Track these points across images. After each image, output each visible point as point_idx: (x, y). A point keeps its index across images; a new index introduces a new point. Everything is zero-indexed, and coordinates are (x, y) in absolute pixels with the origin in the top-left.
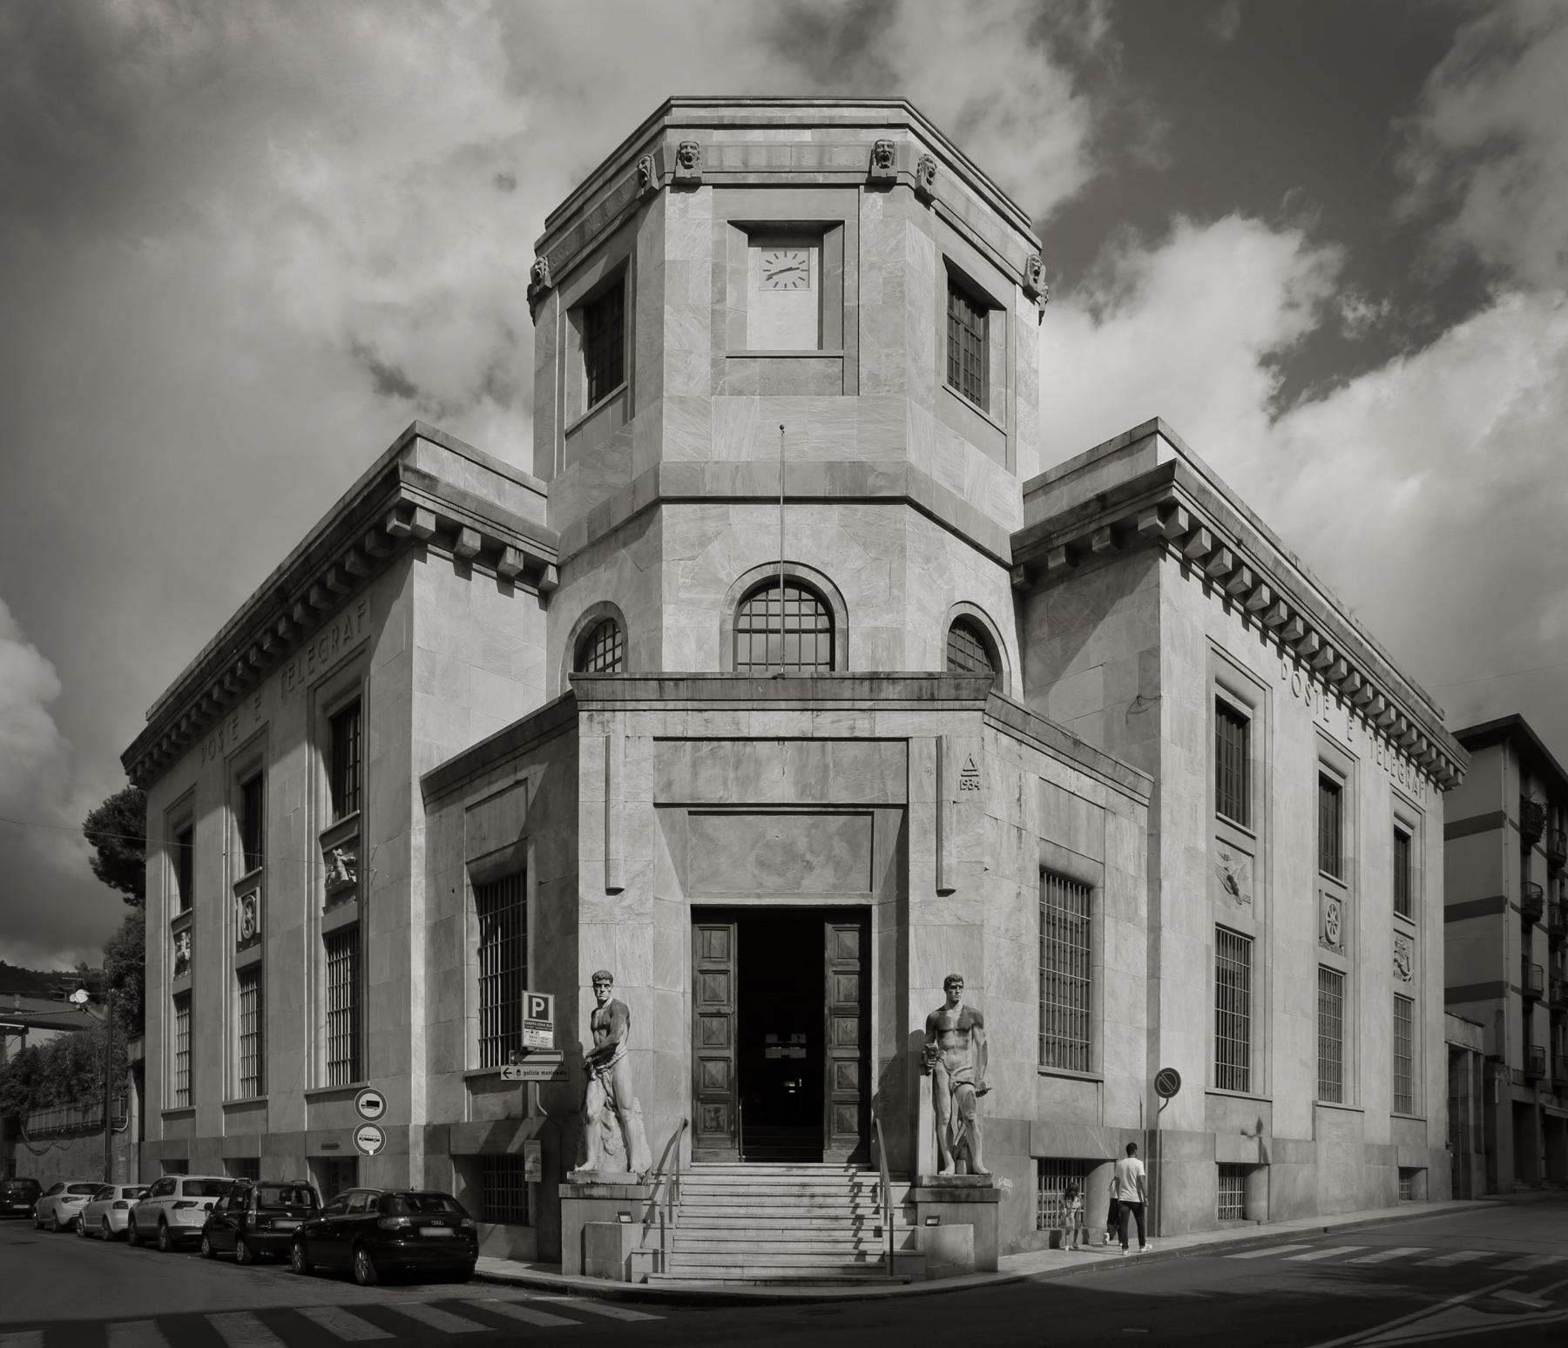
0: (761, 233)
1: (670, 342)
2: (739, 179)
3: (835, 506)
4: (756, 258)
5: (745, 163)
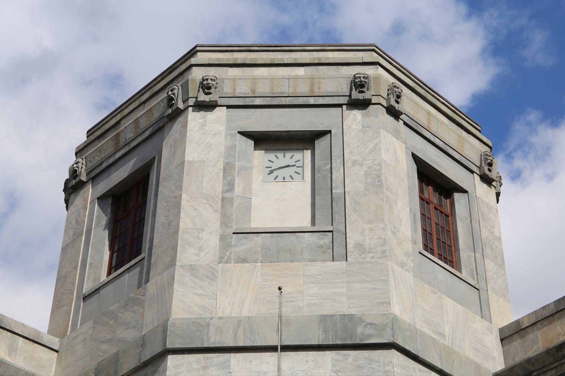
0: (263, 140)
1: (185, 222)
2: (248, 102)
3: (328, 353)
4: (260, 158)
5: (253, 91)
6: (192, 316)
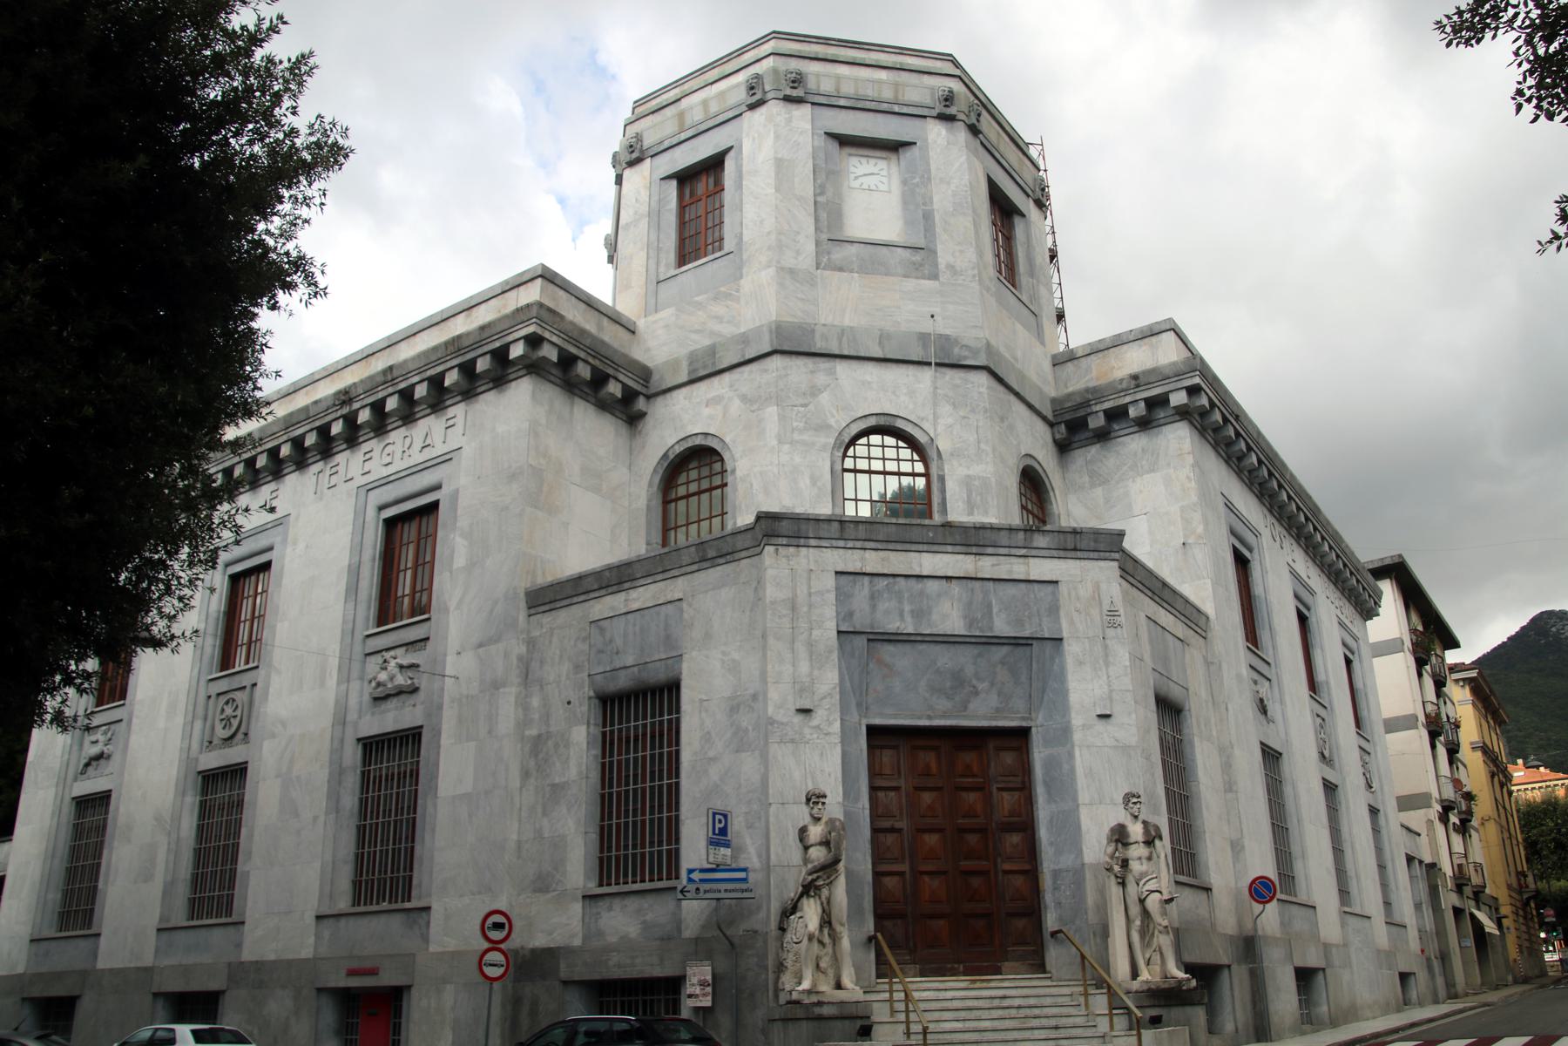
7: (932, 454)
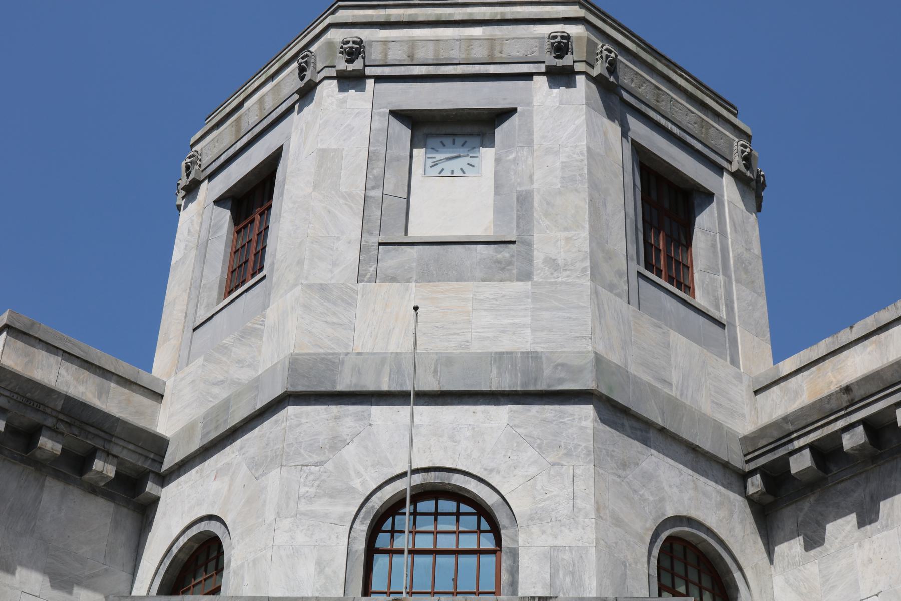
6: (322, 351)
7: (502, 519)
